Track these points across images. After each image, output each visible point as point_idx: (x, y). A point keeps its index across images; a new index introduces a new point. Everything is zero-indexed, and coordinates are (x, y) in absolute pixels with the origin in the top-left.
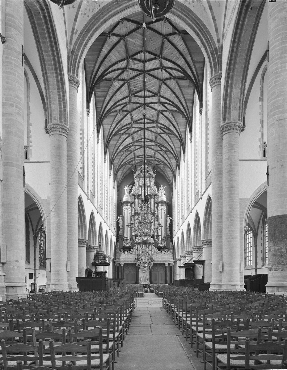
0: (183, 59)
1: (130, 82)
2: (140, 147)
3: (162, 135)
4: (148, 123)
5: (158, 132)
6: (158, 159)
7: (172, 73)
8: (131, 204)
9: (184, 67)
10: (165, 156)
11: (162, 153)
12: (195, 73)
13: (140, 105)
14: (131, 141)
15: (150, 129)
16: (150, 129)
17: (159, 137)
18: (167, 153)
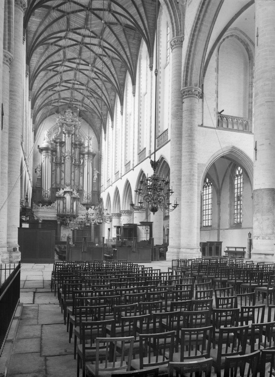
0: (135, 9)
1: (71, 16)
2: (67, 88)
3: (96, 80)
4: (82, 64)
5: (92, 76)
6: (87, 105)
7: (119, 19)
8: (52, 151)
9: (135, 17)
10: (96, 104)
11: (93, 100)
12: (147, 27)
13: (77, 43)
14: (59, 80)
15: (82, 71)
16: (82, 71)
17: (92, 82)
18: (99, 101)
